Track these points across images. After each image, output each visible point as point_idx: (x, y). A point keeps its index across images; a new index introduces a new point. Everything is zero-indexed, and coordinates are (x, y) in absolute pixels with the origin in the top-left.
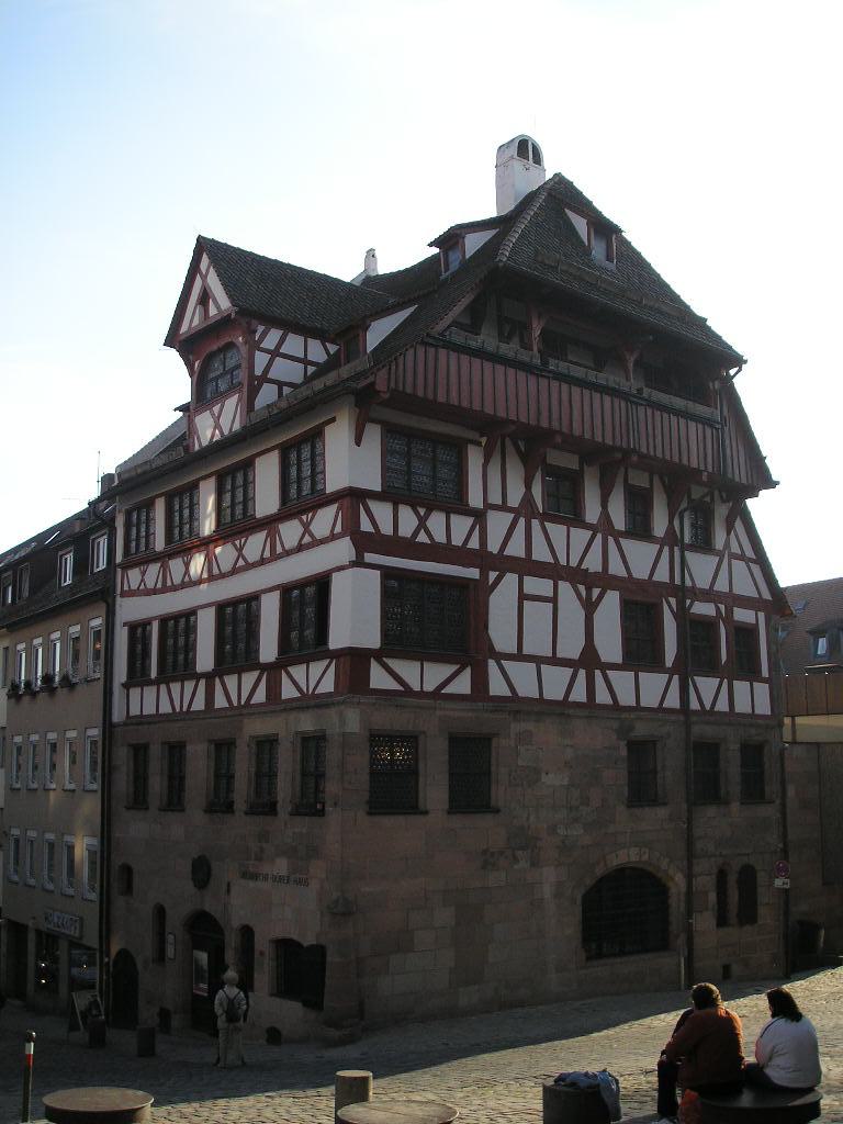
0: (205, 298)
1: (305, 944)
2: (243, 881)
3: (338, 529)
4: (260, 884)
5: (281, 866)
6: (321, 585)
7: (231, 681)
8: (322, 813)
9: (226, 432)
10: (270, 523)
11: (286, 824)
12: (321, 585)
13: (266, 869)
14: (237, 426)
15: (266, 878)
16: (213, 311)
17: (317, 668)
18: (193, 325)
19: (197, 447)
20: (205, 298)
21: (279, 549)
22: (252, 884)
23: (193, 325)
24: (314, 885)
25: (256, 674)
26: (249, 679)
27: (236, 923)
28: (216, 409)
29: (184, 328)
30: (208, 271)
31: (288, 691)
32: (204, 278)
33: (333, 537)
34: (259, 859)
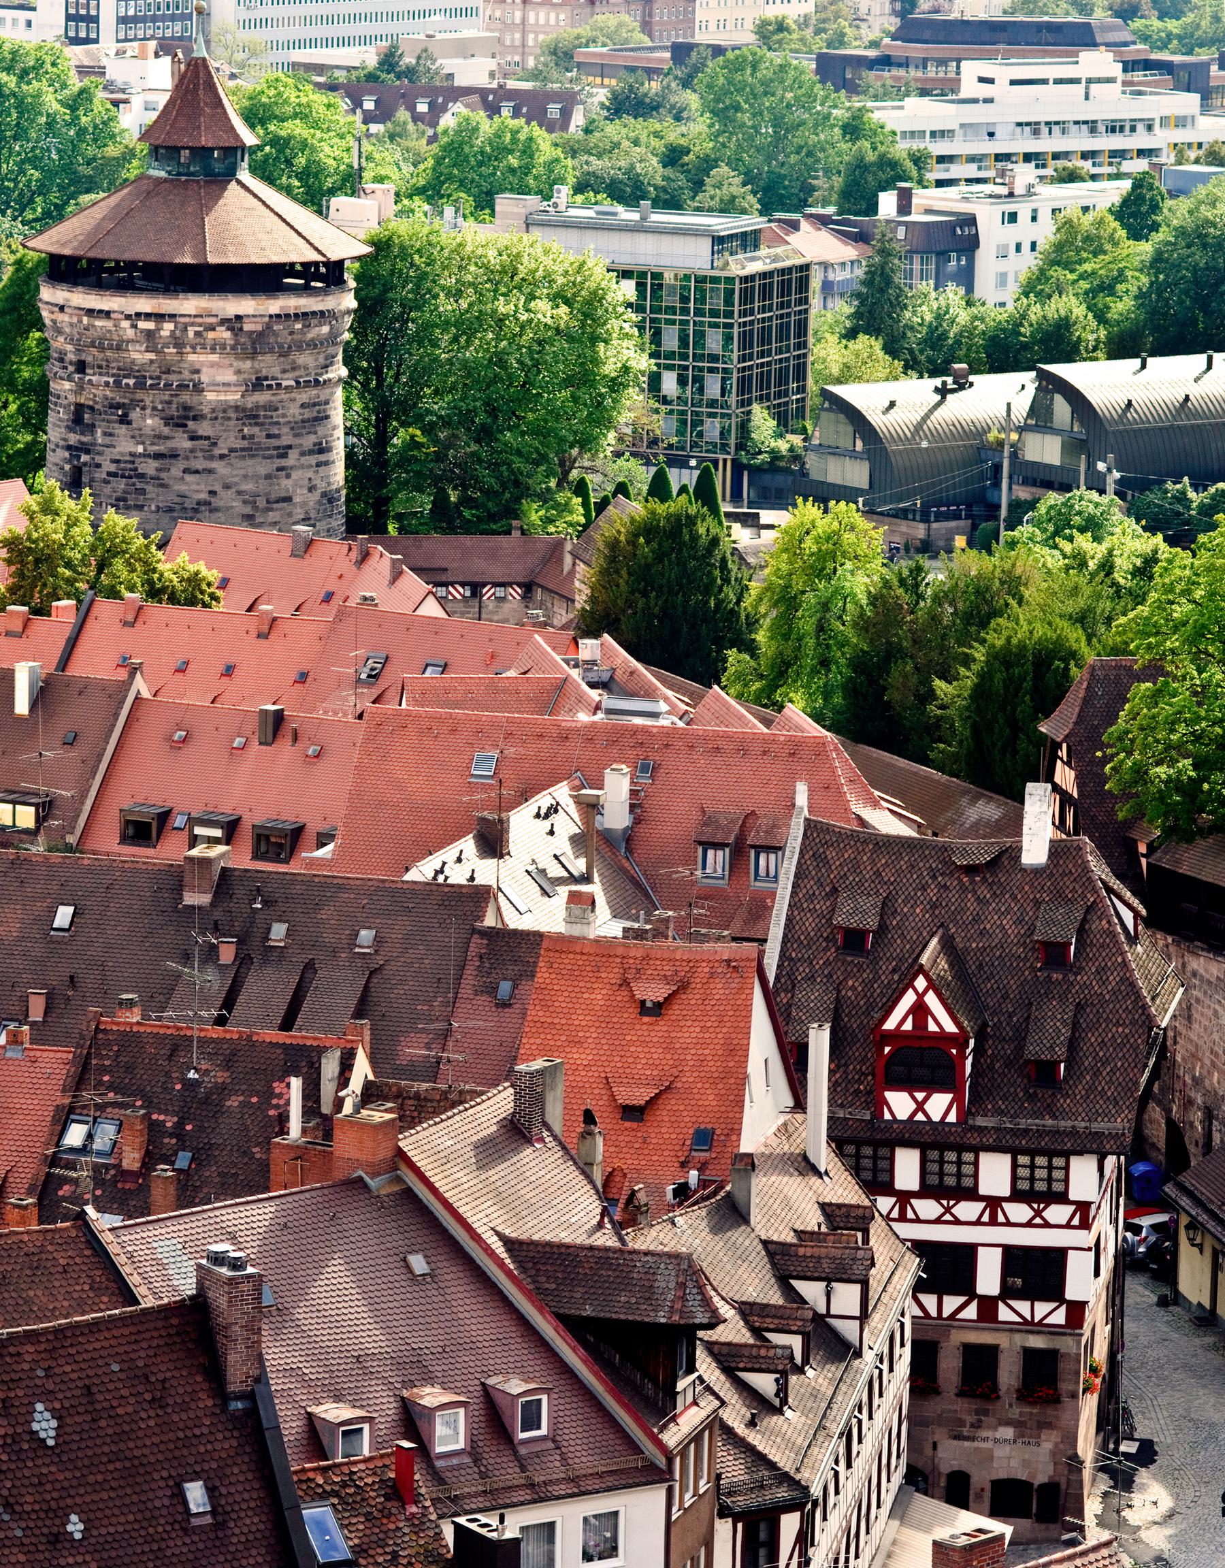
0: (920, 1011)
1: (1036, 1483)
2: (955, 1442)
3: (1076, 1222)
4: (976, 1444)
5: (1008, 1432)
6: (1056, 1259)
7: (930, 1301)
8: (1057, 1401)
9: (936, 1118)
10: (994, 1203)
11: (1011, 1405)
12: (1056, 1259)
13: (984, 1433)
14: (952, 1118)
15: (986, 1439)
16: (932, 1027)
17: (1042, 1308)
18: (904, 1028)
19: (887, 1116)
20: (920, 1011)
21: (1001, 1219)
22: (967, 1444)
23: (904, 1028)
24: (1047, 1446)
25: (962, 1299)
26: (951, 1303)
27: (945, 1469)
28: (920, 1096)
29: (890, 1024)
30: (926, 991)
31: (1004, 1314)
32: (920, 996)
33: (1068, 1226)
34: (977, 1425)
